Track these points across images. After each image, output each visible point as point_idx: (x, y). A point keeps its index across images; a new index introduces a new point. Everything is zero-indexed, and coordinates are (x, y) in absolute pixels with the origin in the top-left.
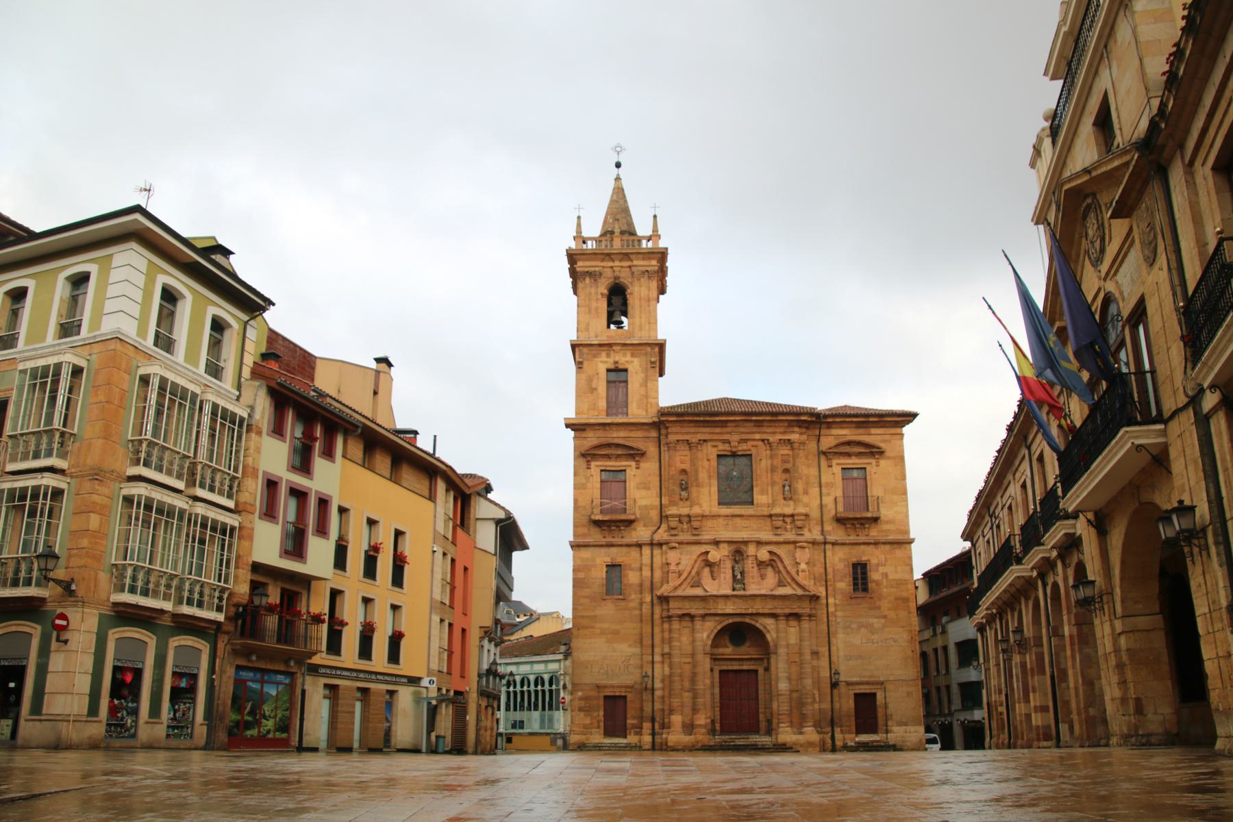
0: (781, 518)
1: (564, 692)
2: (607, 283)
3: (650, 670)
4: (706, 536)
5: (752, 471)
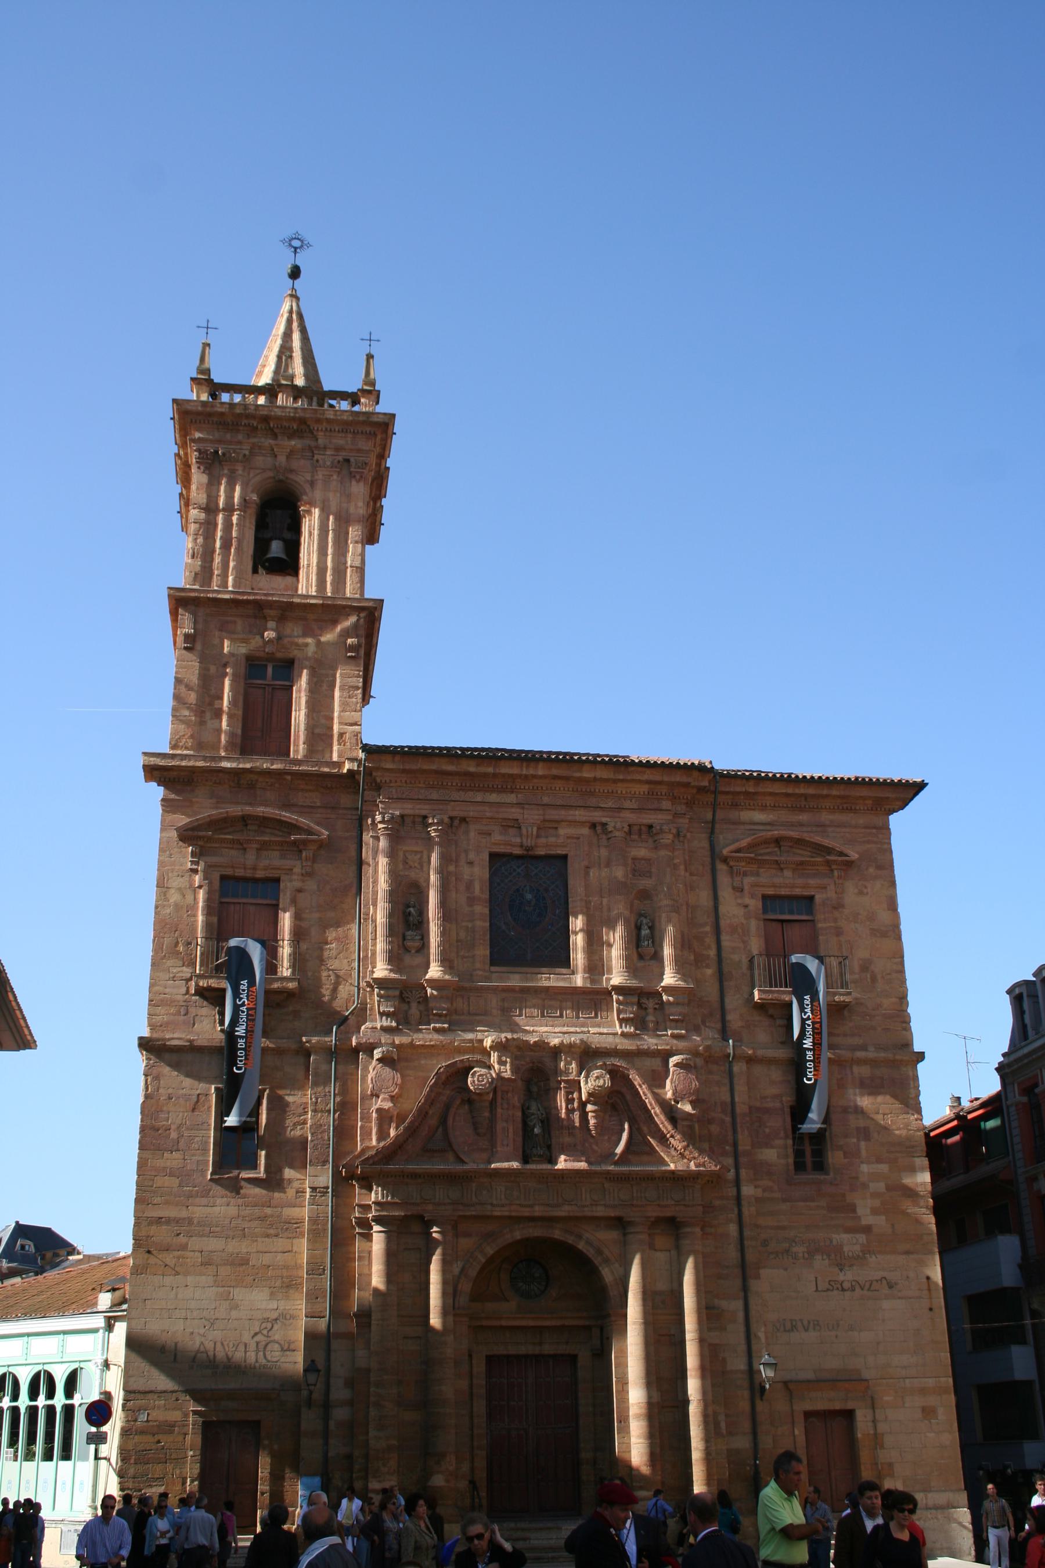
0: (635, 999)
2: (258, 478)
5: (567, 893)
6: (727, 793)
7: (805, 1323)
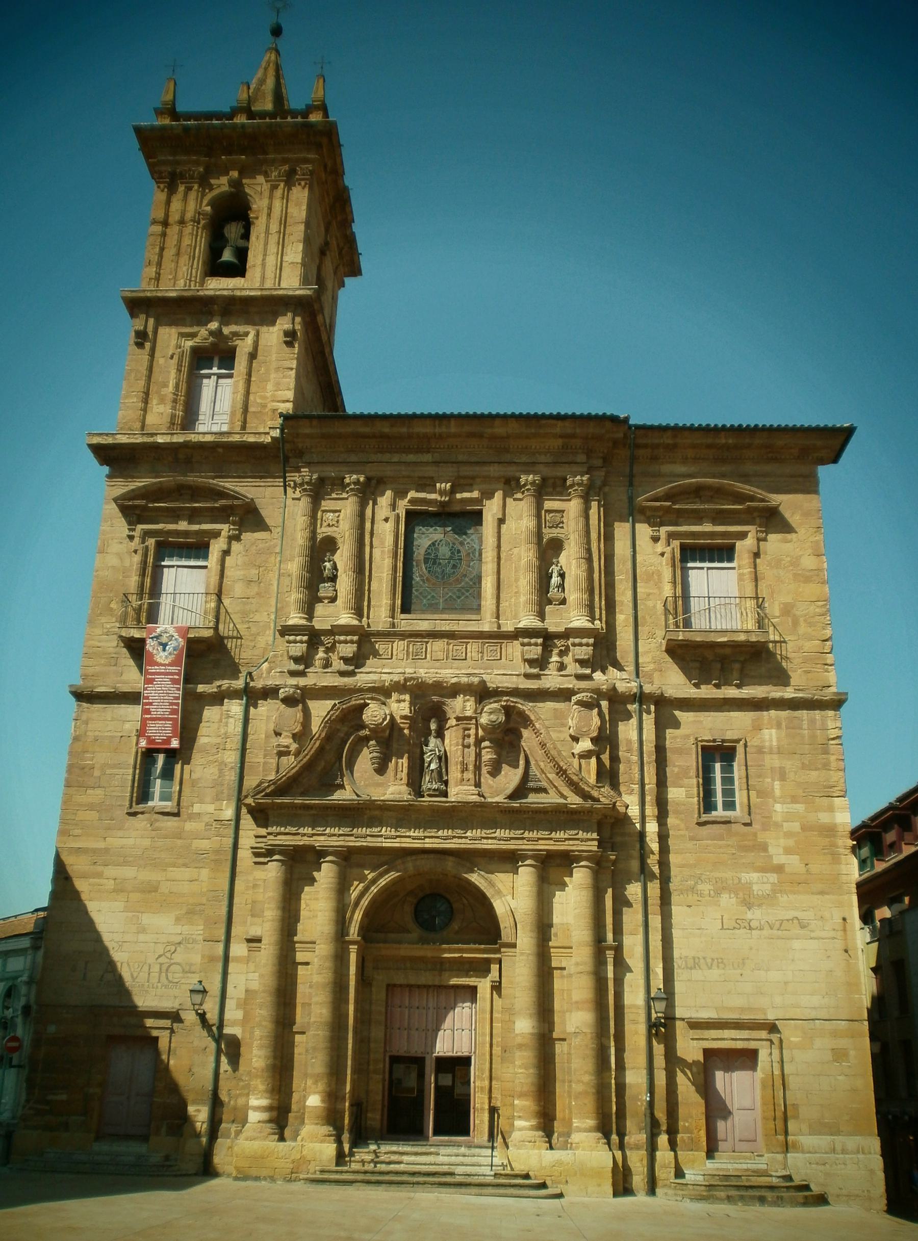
0: (540, 641)
1: (24, 1023)
3: (218, 978)
4: (366, 677)
6: (646, 446)
7: (709, 961)
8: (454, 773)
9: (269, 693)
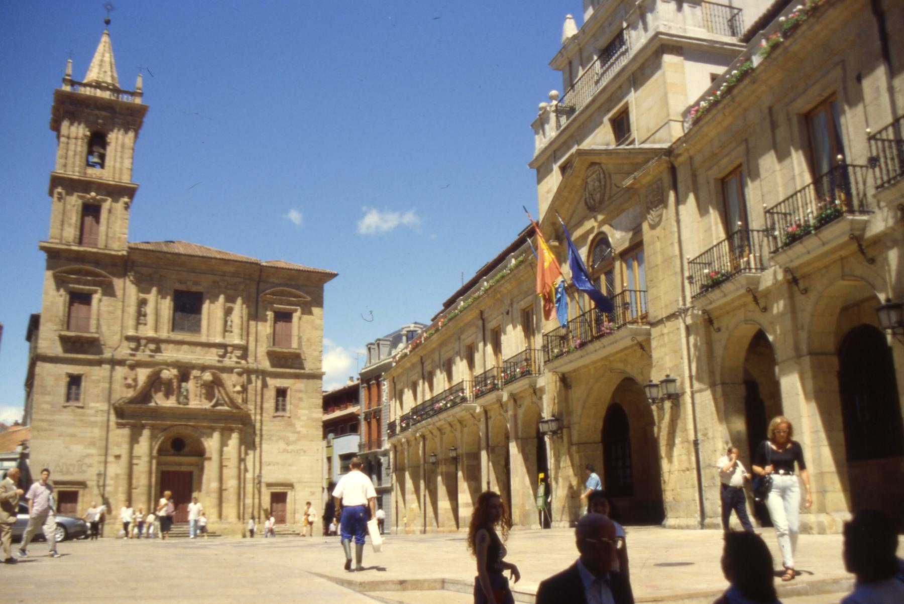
4: (159, 357)
8: (191, 396)
9: (121, 363)
